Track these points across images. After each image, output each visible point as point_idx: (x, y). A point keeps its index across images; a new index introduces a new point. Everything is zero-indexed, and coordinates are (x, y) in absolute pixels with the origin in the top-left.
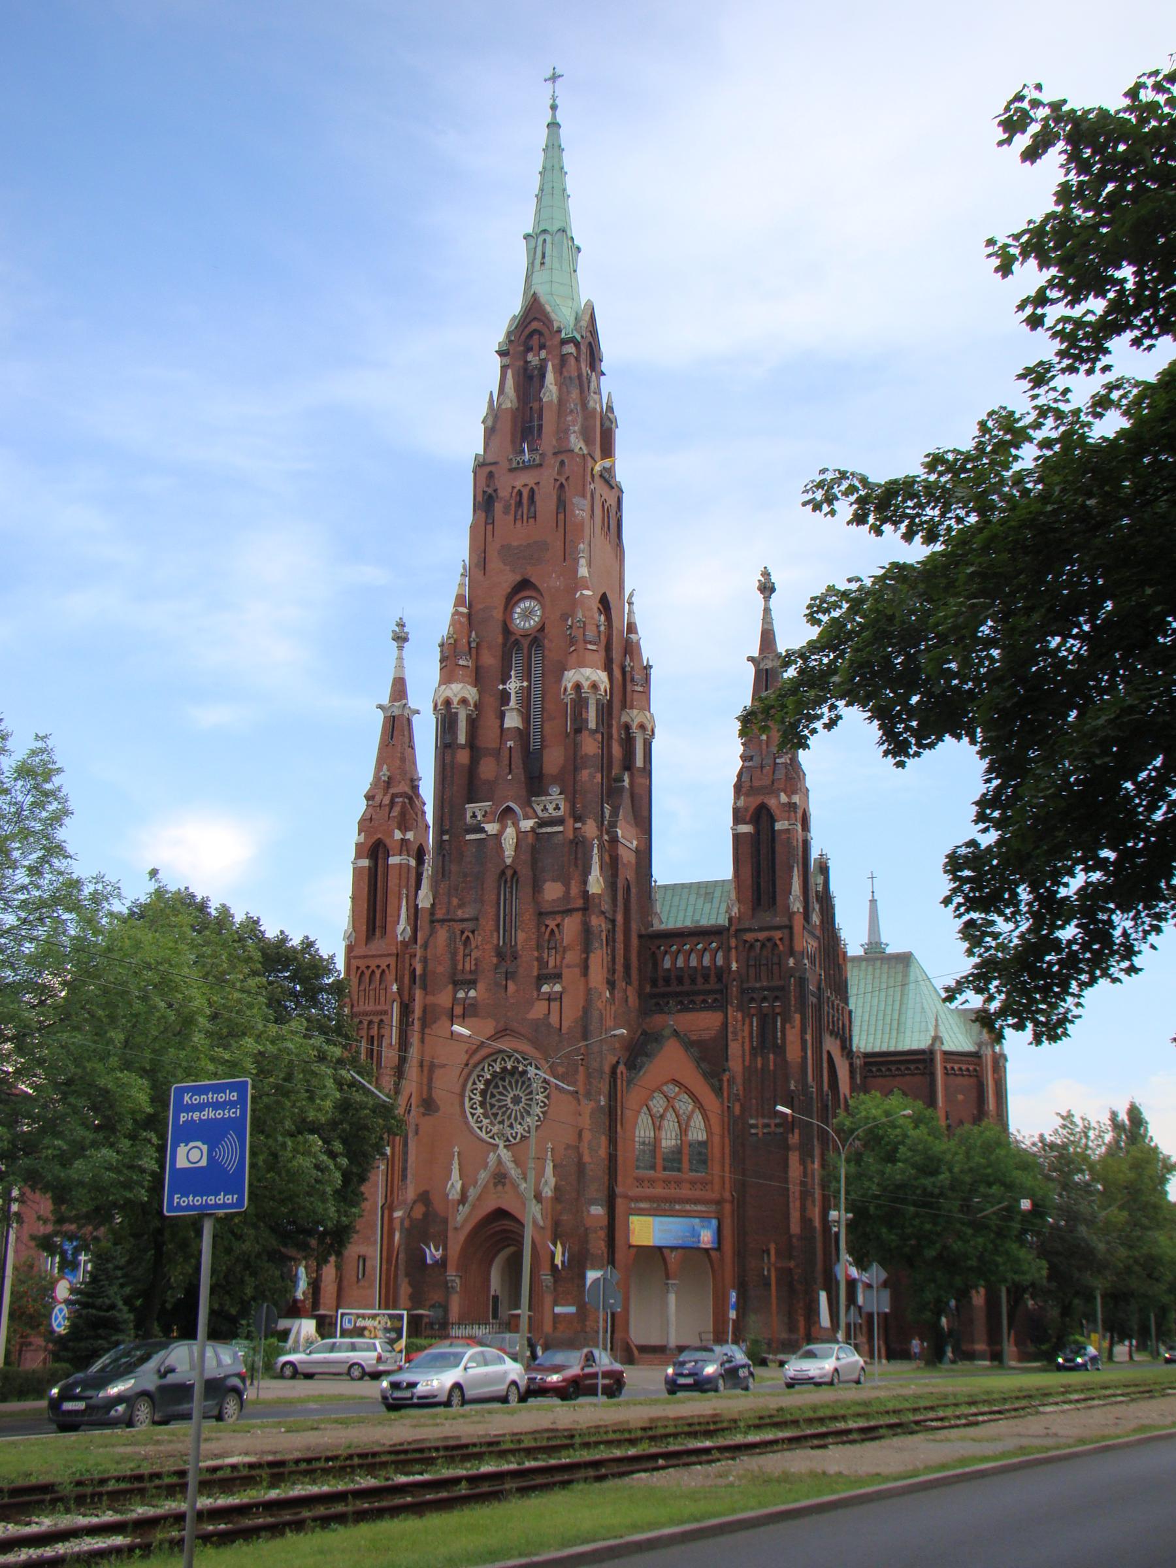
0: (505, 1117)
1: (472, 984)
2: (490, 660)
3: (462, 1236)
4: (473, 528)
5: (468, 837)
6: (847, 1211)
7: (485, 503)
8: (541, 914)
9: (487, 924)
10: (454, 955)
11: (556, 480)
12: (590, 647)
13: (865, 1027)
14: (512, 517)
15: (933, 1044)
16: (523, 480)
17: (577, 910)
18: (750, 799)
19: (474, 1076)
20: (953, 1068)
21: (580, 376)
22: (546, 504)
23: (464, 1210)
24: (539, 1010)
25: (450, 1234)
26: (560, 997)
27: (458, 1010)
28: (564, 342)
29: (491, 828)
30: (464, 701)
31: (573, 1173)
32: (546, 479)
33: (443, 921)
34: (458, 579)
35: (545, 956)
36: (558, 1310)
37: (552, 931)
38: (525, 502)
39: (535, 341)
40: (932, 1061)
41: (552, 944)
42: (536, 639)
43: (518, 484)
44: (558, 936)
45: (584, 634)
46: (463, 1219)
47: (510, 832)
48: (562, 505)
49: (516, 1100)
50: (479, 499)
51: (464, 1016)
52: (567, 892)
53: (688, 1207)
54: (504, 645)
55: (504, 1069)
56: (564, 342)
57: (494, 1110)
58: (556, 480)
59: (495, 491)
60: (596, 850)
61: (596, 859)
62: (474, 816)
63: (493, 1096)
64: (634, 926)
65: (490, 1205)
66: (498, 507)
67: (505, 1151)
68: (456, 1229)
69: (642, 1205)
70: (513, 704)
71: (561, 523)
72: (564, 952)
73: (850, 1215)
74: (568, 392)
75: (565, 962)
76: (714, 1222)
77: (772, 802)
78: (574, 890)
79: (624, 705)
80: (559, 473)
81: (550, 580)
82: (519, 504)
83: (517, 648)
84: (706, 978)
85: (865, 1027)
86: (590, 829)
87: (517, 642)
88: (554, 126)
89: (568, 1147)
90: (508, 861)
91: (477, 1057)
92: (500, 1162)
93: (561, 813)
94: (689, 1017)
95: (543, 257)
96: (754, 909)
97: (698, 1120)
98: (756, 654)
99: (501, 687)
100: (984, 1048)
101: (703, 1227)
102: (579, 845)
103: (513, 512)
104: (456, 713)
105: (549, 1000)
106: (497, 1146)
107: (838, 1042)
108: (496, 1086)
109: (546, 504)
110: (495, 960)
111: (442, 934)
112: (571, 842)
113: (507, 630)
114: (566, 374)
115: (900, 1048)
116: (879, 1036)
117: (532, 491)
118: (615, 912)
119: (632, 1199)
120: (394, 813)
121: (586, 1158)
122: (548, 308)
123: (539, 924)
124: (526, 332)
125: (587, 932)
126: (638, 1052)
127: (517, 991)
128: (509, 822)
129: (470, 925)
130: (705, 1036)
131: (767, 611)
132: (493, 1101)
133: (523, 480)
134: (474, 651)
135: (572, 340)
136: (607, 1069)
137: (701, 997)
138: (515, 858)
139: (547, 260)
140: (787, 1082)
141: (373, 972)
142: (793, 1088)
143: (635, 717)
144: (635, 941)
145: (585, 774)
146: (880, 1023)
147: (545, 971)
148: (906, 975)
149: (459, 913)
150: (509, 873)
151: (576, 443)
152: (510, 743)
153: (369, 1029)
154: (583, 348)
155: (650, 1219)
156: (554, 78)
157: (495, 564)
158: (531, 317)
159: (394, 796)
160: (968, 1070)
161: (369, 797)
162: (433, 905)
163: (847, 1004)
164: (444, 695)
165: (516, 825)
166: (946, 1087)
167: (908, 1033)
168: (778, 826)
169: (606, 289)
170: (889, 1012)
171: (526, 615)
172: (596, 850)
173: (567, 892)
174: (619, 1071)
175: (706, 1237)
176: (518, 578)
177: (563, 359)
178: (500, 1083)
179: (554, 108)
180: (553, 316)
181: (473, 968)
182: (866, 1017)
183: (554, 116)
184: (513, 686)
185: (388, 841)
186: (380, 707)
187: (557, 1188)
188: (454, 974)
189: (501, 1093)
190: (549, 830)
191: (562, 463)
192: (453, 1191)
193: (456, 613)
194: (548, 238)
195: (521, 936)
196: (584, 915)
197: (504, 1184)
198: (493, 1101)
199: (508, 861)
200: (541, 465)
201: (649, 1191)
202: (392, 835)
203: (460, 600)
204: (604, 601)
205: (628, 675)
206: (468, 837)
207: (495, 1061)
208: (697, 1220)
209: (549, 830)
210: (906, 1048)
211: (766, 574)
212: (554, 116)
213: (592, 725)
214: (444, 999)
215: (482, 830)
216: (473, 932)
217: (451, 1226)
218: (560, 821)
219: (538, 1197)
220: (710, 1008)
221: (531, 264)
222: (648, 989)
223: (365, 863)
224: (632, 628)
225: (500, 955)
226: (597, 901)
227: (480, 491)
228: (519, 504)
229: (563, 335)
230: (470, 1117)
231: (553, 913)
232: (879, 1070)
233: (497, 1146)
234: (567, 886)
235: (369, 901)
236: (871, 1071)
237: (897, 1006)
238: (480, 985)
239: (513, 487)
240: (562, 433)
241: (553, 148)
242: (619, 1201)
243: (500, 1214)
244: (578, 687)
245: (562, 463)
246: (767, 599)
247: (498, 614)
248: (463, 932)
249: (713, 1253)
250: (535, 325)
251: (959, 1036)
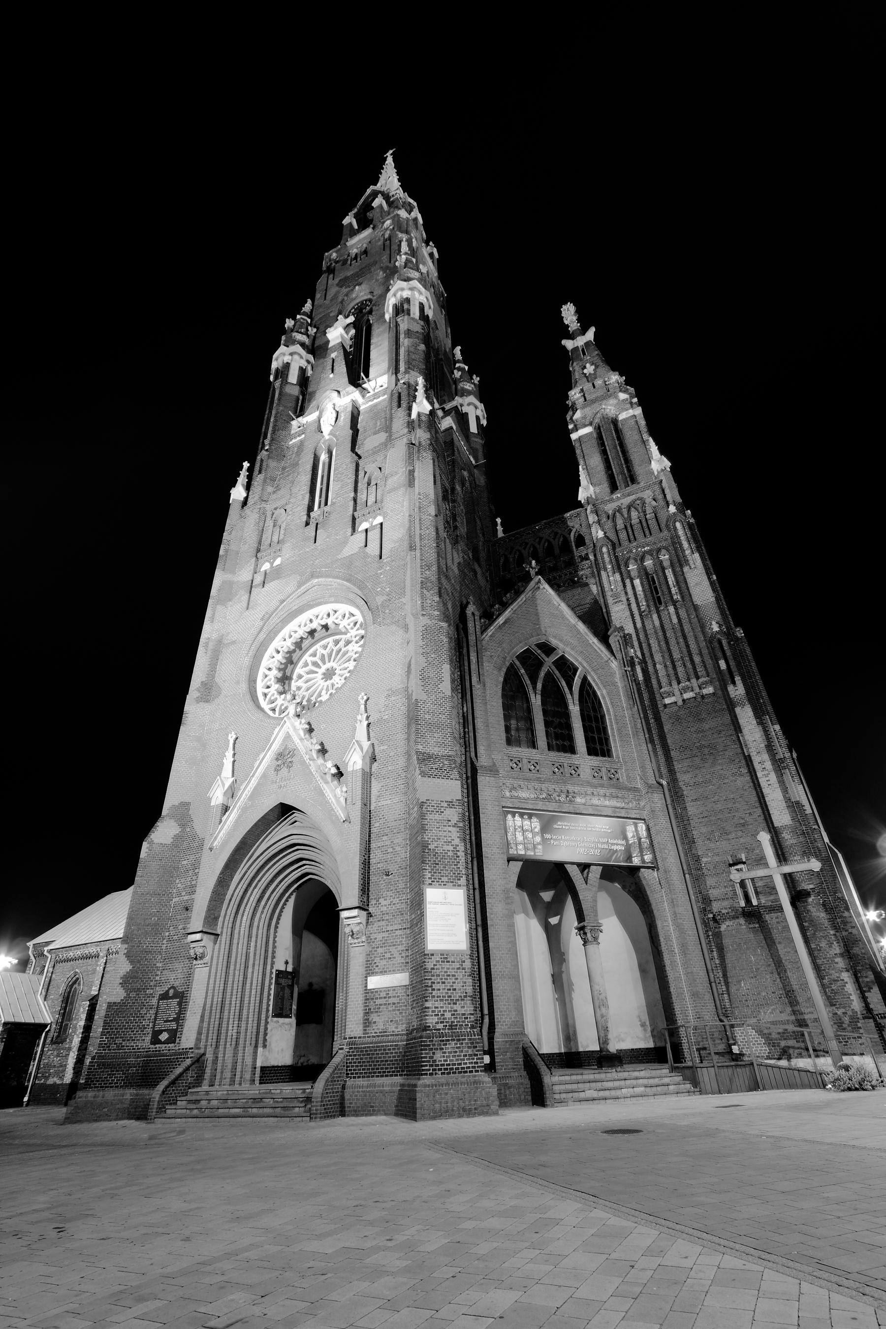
18: (587, 410)
27: (259, 579)
36: (374, 982)
89: (392, 692)
92: (288, 737)
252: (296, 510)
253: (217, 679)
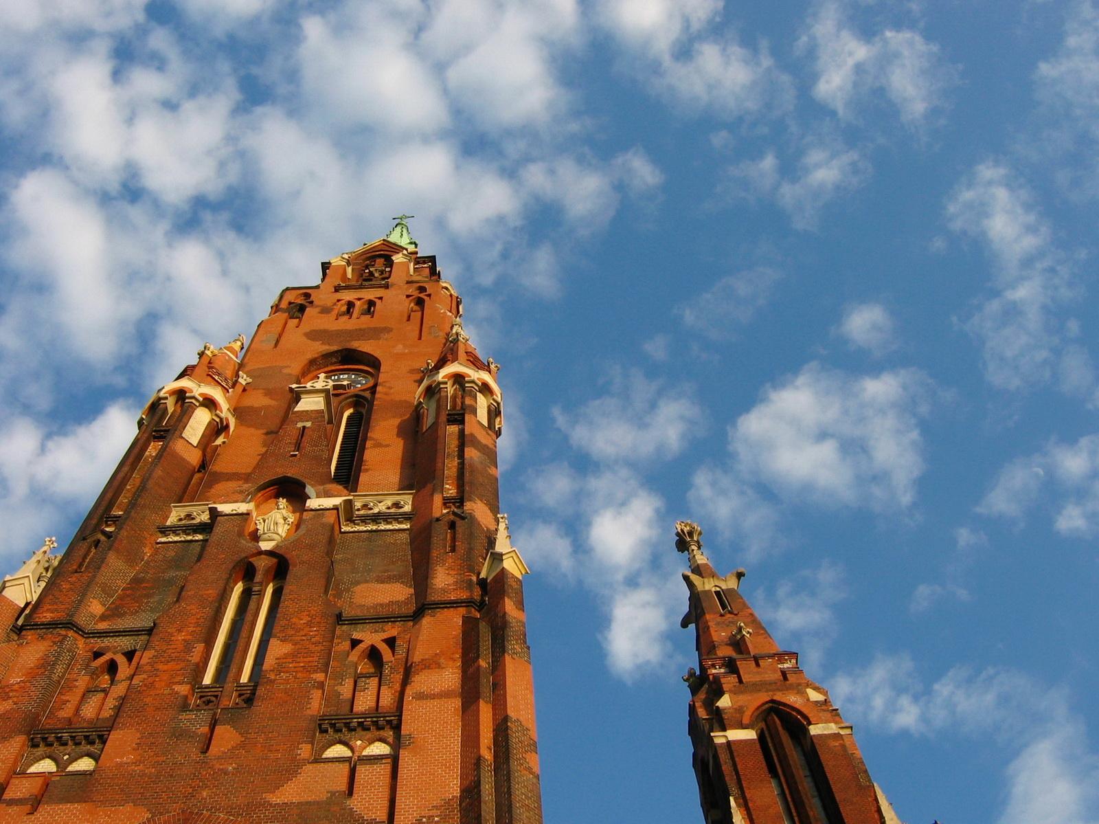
8: (339, 618)
77: (793, 699)
127: (242, 745)
216: (130, 655)
231: (379, 619)
252: (161, 667)
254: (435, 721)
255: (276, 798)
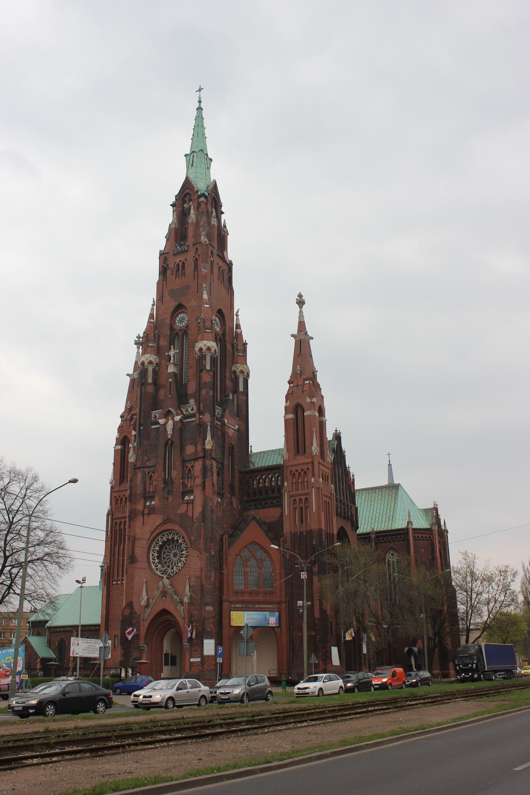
0: (170, 564)
1: (152, 498)
2: (163, 343)
3: (146, 624)
4: (158, 283)
5: (152, 427)
6: (307, 601)
7: (163, 271)
8: (184, 461)
9: (160, 469)
10: (145, 484)
11: (194, 257)
12: (207, 331)
13: (377, 520)
14: (174, 276)
15: (408, 525)
16: (178, 259)
17: (200, 458)
19: (154, 543)
20: (418, 537)
21: (207, 211)
22: (190, 268)
23: (148, 610)
24: (182, 509)
25: (141, 623)
26: (192, 502)
27: (146, 511)
28: (199, 197)
29: (162, 421)
30: (150, 362)
31: (199, 590)
32: (190, 257)
33: (140, 468)
34: (151, 307)
35: (186, 482)
36: (192, 660)
37: (189, 469)
38: (181, 268)
39: (187, 199)
40: (408, 533)
41: (190, 476)
42: (185, 331)
43: (177, 261)
44: (192, 472)
45: (204, 325)
46: (147, 616)
47: (170, 422)
48: (196, 267)
49: (175, 555)
50: (161, 270)
51: (149, 514)
52: (196, 450)
53: (262, 606)
54: (171, 335)
55: (168, 539)
56: (199, 197)
57: (165, 560)
58: (194, 257)
59: (168, 265)
60: (209, 428)
61: (209, 432)
62: (155, 417)
63: (165, 553)
64: (236, 467)
65: (159, 608)
66: (169, 272)
67: (167, 580)
68: (143, 620)
69: (238, 606)
70: (172, 361)
71: (196, 276)
72: (195, 479)
73: (309, 603)
74: (201, 218)
75: (195, 484)
76: (277, 614)
78: (199, 448)
79: (234, 362)
80: (196, 253)
81: (191, 303)
82: (178, 270)
83: (178, 336)
84: (273, 491)
85: (377, 520)
86: (207, 418)
87: (177, 334)
88: (200, 109)
90: (169, 437)
91: (155, 534)
92: (164, 586)
93: (194, 411)
94: (265, 511)
95: (193, 163)
96: (295, 455)
97: (267, 563)
98: (295, 332)
99: (167, 354)
100: (433, 526)
101: (271, 616)
102: (201, 426)
103: (175, 274)
104: (147, 368)
105: (188, 503)
106: (163, 577)
107: (349, 522)
108: (166, 549)
109: (190, 268)
110: (163, 486)
111: (139, 475)
112: (198, 424)
113: (172, 328)
114: (200, 210)
115: (393, 528)
116: (383, 523)
117: (183, 263)
118: (223, 459)
119: (231, 603)
120: (132, 423)
121: (204, 582)
122: (193, 183)
123: (183, 466)
124: (183, 195)
125: (205, 470)
126: (236, 529)
128: (170, 418)
129: (152, 469)
130: (273, 520)
131: (301, 312)
132: (165, 556)
133: (178, 259)
134: (157, 339)
135: (203, 195)
136: (218, 537)
137: (271, 501)
138: (172, 435)
139: (194, 164)
140: (312, 541)
141: (122, 498)
142: (314, 543)
143: (238, 367)
144: (237, 475)
145: (204, 392)
146: (384, 517)
147: (186, 489)
148: (397, 494)
149: (148, 464)
150: (170, 442)
151: (204, 239)
152: (170, 380)
153: (120, 525)
154: (210, 199)
155: (242, 612)
156: (200, 90)
157: (167, 298)
158: (185, 188)
159: (133, 415)
160: (426, 537)
161: (122, 417)
162: (136, 460)
163: (355, 504)
164: (141, 361)
165: (173, 419)
166: (415, 546)
167: (397, 521)
168: (306, 414)
169: (223, 174)
170: (388, 512)
171: (181, 321)
172: (209, 428)
173: (196, 450)
174: (224, 539)
175: (273, 620)
176: (177, 304)
177: (199, 204)
178: (168, 547)
179: (200, 102)
180: (195, 186)
181: (153, 490)
182: (378, 515)
183: (200, 105)
184: (172, 353)
185: (129, 436)
186: (128, 375)
187: (191, 598)
188: (145, 494)
189: (168, 552)
190: (189, 420)
191: (197, 249)
192: (143, 601)
193: (149, 322)
194: (195, 154)
195: (174, 473)
196: (204, 460)
197: (166, 597)
198: (165, 556)
199: (169, 437)
200: (187, 251)
201: (241, 598)
202: (131, 433)
203: (151, 316)
204: (220, 312)
205: (235, 348)
206: (152, 427)
207: (164, 535)
208: (268, 613)
209: (189, 420)
210: (396, 528)
211: (300, 296)
212: (200, 105)
213: (208, 367)
214: (140, 507)
215: (158, 423)
216: (153, 473)
217: (141, 619)
218: (194, 416)
219: (182, 603)
220: (275, 506)
221: (188, 167)
222: (245, 498)
223: (119, 447)
224: (238, 326)
225: (165, 482)
226: (209, 452)
227: (161, 266)
228: (178, 270)
229: (199, 193)
230: (152, 564)
232: (383, 539)
233: (163, 577)
234: (196, 446)
235: (121, 467)
236: (379, 540)
237: (392, 508)
238: (156, 499)
239: (175, 263)
240: (197, 235)
241: (199, 118)
242: (225, 604)
243: (164, 612)
244: (201, 349)
245: (197, 249)
246: (301, 307)
247: (168, 321)
248: (149, 473)
249: (276, 629)
250: (187, 191)
251: (422, 522)
252: (159, 479)
253: (135, 554)
254: (198, 492)
255: (178, 512)
